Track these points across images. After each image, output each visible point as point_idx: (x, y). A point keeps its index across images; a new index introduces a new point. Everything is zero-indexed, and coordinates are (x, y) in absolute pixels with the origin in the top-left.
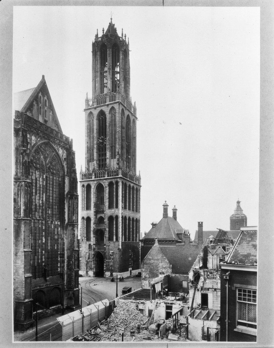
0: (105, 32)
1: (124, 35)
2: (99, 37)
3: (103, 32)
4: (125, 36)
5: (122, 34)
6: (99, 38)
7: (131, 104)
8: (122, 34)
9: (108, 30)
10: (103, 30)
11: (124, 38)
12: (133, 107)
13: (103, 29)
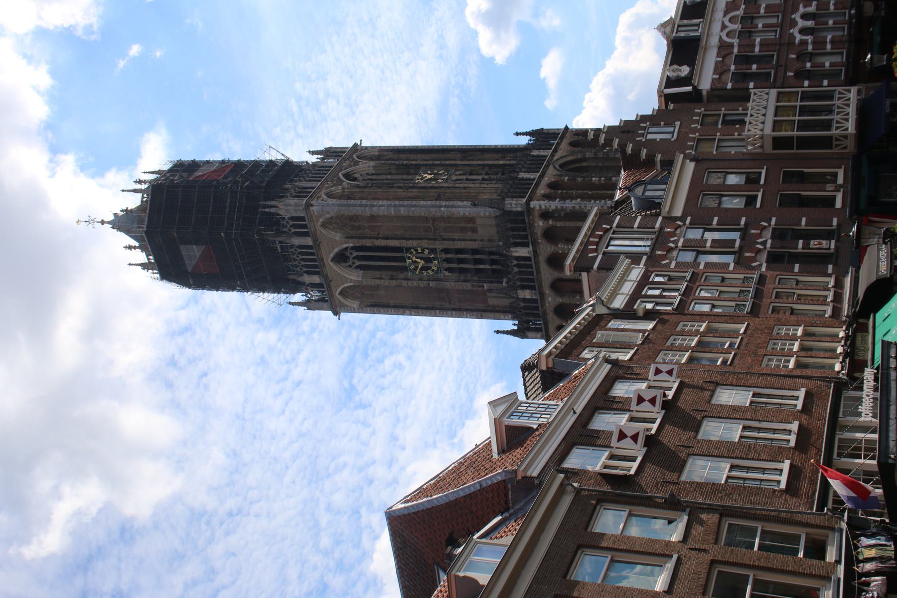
0: (135, 243)
1: (138, 186)
2: (146, 261)
3: (135, 248)
4: (140, 182)
5: (135, 191)
6: (149, 259)
7: (314, 165)
8: (135, 191)
9: (128, 232)
10: (130, 247)
11: (144, 186)
12: (323, 159)
13: (126, 247)
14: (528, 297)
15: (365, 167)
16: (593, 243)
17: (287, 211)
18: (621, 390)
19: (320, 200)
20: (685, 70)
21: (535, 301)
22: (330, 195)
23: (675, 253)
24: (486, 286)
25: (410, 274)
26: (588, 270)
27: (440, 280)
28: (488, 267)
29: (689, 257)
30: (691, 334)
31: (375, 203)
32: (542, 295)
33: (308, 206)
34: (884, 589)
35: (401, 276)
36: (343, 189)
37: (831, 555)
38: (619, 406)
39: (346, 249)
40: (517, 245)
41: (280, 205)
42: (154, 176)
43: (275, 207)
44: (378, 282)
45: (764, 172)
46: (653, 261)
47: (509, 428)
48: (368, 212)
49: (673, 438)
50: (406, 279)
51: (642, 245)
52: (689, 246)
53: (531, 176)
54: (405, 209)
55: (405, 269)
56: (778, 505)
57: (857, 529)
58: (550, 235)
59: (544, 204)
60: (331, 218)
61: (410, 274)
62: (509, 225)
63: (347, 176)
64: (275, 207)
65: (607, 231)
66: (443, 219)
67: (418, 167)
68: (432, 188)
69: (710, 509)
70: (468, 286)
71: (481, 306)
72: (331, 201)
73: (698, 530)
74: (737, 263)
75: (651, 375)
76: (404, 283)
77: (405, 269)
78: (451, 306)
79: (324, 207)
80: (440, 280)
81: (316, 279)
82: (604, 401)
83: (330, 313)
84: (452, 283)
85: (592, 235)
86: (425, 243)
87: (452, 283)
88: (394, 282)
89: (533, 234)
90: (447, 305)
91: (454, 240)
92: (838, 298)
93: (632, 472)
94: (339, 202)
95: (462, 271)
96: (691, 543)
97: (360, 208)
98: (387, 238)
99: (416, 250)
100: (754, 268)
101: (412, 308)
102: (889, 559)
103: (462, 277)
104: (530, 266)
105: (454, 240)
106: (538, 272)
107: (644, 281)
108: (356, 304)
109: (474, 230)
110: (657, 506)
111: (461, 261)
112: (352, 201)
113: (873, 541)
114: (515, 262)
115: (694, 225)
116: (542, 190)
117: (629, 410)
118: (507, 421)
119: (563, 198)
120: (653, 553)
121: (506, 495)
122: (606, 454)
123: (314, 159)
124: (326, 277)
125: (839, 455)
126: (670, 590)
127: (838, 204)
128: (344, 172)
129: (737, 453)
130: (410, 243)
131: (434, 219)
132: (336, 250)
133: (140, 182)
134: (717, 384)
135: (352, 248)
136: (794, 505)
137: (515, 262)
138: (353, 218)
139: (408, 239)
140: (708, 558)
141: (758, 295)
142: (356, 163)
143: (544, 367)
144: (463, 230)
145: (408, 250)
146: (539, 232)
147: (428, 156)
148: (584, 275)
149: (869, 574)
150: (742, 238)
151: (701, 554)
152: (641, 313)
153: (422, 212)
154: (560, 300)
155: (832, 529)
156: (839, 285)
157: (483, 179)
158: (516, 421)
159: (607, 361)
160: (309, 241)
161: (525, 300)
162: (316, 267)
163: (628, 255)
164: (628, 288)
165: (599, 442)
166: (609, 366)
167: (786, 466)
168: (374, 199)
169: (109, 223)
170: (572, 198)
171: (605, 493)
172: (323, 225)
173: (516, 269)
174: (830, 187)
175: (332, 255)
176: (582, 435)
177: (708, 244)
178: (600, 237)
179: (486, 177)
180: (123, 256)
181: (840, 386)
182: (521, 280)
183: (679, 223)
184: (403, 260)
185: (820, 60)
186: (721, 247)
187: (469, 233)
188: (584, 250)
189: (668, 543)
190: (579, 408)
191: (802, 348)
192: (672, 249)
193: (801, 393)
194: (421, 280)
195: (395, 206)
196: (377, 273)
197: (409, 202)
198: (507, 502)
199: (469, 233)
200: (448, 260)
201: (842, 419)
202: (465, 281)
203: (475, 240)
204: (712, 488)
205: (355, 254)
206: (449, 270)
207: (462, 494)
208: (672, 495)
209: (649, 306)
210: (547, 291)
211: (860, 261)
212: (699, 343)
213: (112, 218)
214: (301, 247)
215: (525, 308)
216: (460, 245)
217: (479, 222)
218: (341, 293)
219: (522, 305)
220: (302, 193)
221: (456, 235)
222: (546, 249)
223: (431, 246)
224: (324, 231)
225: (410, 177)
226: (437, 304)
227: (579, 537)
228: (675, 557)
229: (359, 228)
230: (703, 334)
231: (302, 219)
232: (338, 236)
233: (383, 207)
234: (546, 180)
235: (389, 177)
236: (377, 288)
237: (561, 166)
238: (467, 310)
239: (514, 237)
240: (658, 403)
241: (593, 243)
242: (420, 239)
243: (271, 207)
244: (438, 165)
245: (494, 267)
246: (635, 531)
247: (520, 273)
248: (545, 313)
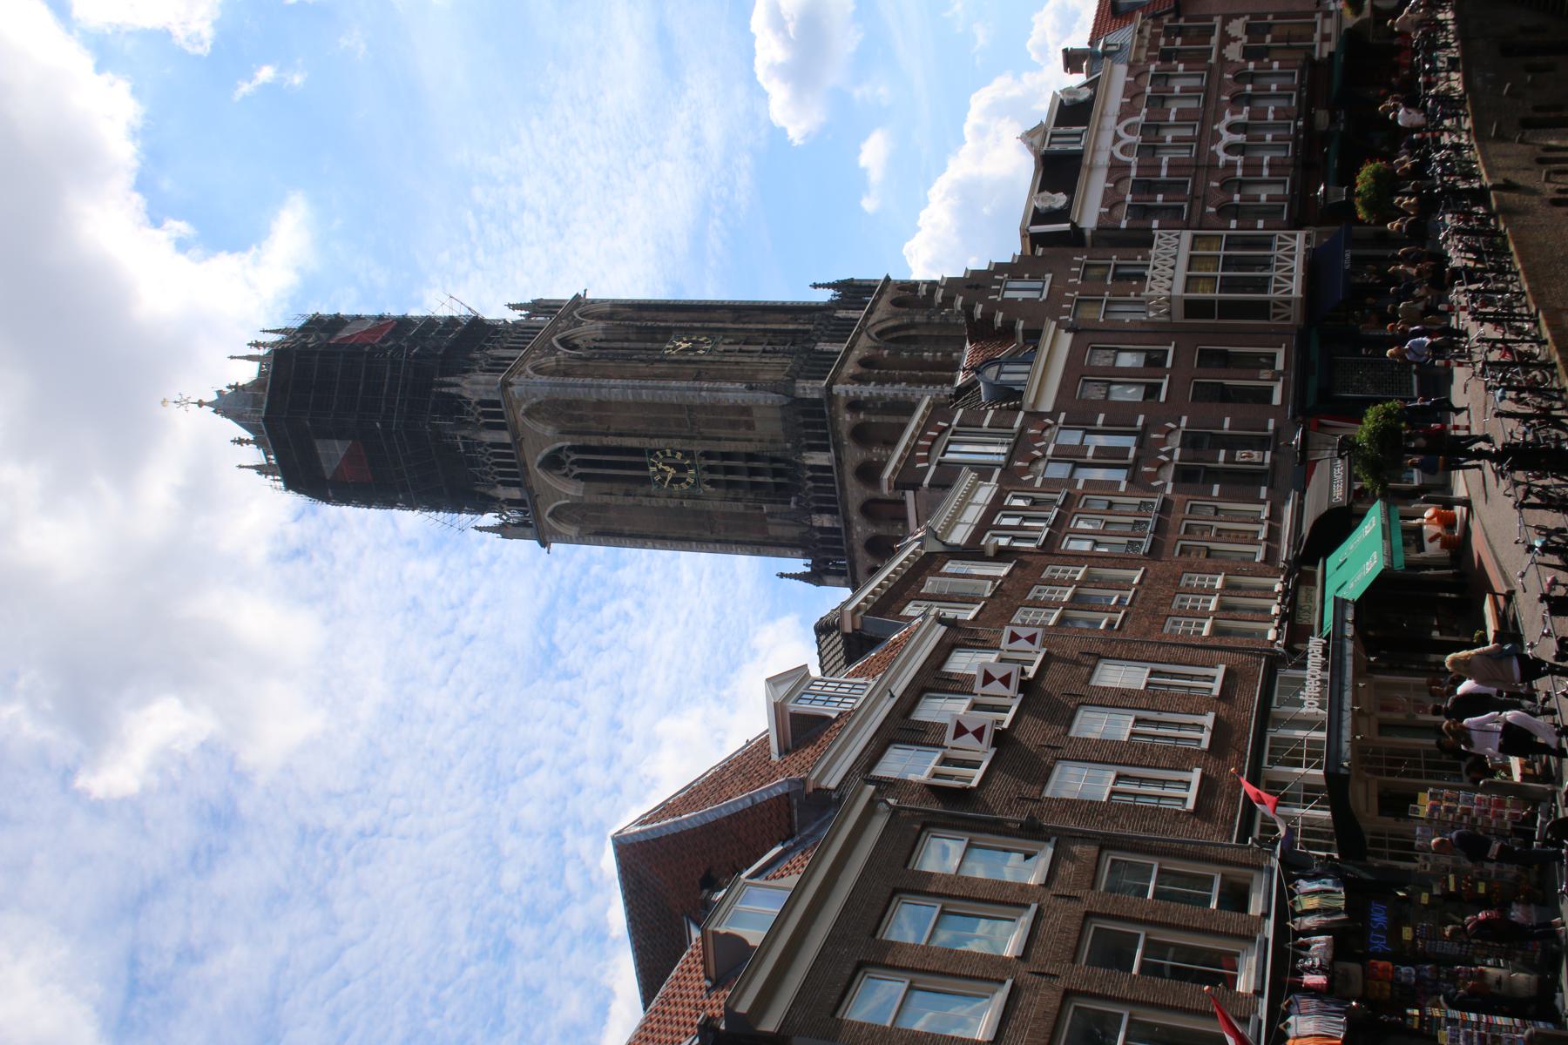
0: (248, 436)
1: (255, 352)
2: (264, 462)
3: (248, 442)
4: (257, 345)
5: (250, 358)
7: (516, 324)
8: (250, 358)
9: (238, 418)
10: (240, 442)
11: (262, 352)
12: (528, 316)
14: (827, 524)
16: (923, 448)
17: (474, 392)
18: (963, 663)
19: (523, 377)
20: (1060, 200)
22: (538, 370)
23: (1041, 465)
24: (765, 508)
25: (654, 487)
26: (916, 486)
27: (697, 498)
28: (769, 480)
29: (1059, 471)
30: (1063, 583)
31: (605, 382)
32: (848, 522)
33: (506, 385)
34: (1329, 954)
35: (641, 490)
36: (558, 361)
37: (1256, 906)
38: (958, 686)
39: (561, 449)
40: (812, 448)
42: (277, 337)
43: (457, 385)
44: (606, 499)
45: (1171, 350)
46: (1010, 477)
47: (795, 717)
48: (594, 396)
49: (1034, 734)
50: (648, 495)
51: (996, 452)
52: (1062, 454)
53: (834, 347)
54: (650, 391)
55: (647, 480)
56: (1182, 834)
57: (1295, 867)
58: (861, 435)
59: (853, 389)
60: (539, 403)
61: (654, 487)
62: (801, 420)
63: (564, 342)
64: (457, 385)
65: (943, 430)
66: (703, 407)
67: (668, 331)
68: (689, 362)
69: (1085, 838)
70: (739, 507)
71: (756, 537)
72: (538, 379)
73: (1068, 869)
74: (1131, 480)
75: (1004, 643)
76: (646, 501)
77: (647, 480)
78: (714, 536)
79: (529, 386)
80: (697, 498)
81: (516, 493)
82: (934, 680)
83: (535, 543)
84: (717, 503)
85: (922, 436)
86: (676, 443)
87: (715, 502)
88: (630, 500)
90: (707, 534)
91: (719, 439)
92: (1274, 534)
93: (974, 784)
94: (551, 380)
95: (730, 485)
96: (1057, 888)
97: (580, 388)
98: (621, 435)
99: (664, 453)
100: (1155, 490)
101: (657, 538)
102: (1337, 911)
103: (731, 494)
104: (831, 480)
105: (719, 439)
106: (842, 484)
107: (996, 505)
108: (573, 531)
109: (750, 426)
110: (1008, 833)
111: (729, 470)
112: (571, 380)
113: (1315, 886)
114: (810, 474)
115: (1069, 424)
116: (850, 368)
117: (971, 694)
118: (793, 707)
119: (881, 381)
120: (1001, 900)
121: (790, 816)
122: (937, 756)
123: (515, 316)
124: (530, 490)
125: (1271, 761)
126: (1024, 956)
127: (1277, 399)
128: (559, 336)
129: (1126, 757)
131: (691, 408)
132: (546, 451)
133: (257, 345)
134: (1099, 657)
135: (573, 449)
136: (1207, 833)
137: (810, 474)
138: (569, 404)
139: (652, 437)
140: (1081, 908)
141: (1160, 528)
142: (578, 324)
143: (848, 629)
144: (733, 425)
145: (652, 452)
146: (845, 431)
147: (683, 316)
148: (910, 494)
149: (1308, 932)
150: (1139, 446)
151: (1072, 904)
152: (991, 552)
154: (873, 530)
155: (1259, 868)
156: (1275, 516)
157: (764, 351)
158: (805, 707)
159: (940, 620)
160: (505, 437)
161: (822, 529)
162: (516, 475)
163: (974, 466)
164: (973, 514)
165: (927, 739)
166: (944, 629)
167: (1195, 776)
168: (603, 376)
169: (210, 404)
170: (894, 381)
171: (934, 813)
172: (527, 414)
173: (811, 484)
174: (1265, 374)
175: (539, 458)
176: (904, 728)
177: (1090, 453)
178: (934, 440)
179: (769, 348)
180: (234, 452)
181: (1274, 663)
183: (1048, 421)
184: (644, 467)
185: (1252, 191)
186: (1108, 458)
187: (742, 430)
188: (909, 460)
189: (1024, 888)
190: (899, 689)
191: (1222, 607)
192: (1037, 459)
193: (1219, 672)
194: (670, 497)
195: (633, 388)
196: (605, 486)
197: (655, 383)
198: (790, 825)
199: (742, 430)
200: (710, 469)
201: (1276, 709)
202: (736, 500)
203: (750, 440)
204: (1089, 808)
205: (574, 457)
206: (712, 483)
207: (725, 813)
208: (1031, 818)
209: (1003, 542)
211: (1306, 482)
212: (1074, 596)
213: (215, 397)
214: (493, 445)
215: (822, 541)
217: (757, 413)
218: (552, 515)
219: (818, 536)
220: (497, 365)
221: (722, 433)
222: (855, 455)
223: (685, 448)
224: (528, 423)
225: (656, 345)
226: (693, 533)
227: (895, 878)
228: (1034, 907)
229: (581, 419)
230: (1081, 584)
231: (496, 404)
232: (549, 430)
233: (615, 389)
234: (856, 354)
235: (626, 344)
236: (605, 507)
237: (880, 334)
238: (737, 543)
239: (808, 436)
240: (1014, 682)
241: (923, 448)
242: (670, 437)
243: (451, 385)
244: (697, 329)
245: (778, 480)
246: (981, 868)
247: (816, 489)
248: (851, 550)
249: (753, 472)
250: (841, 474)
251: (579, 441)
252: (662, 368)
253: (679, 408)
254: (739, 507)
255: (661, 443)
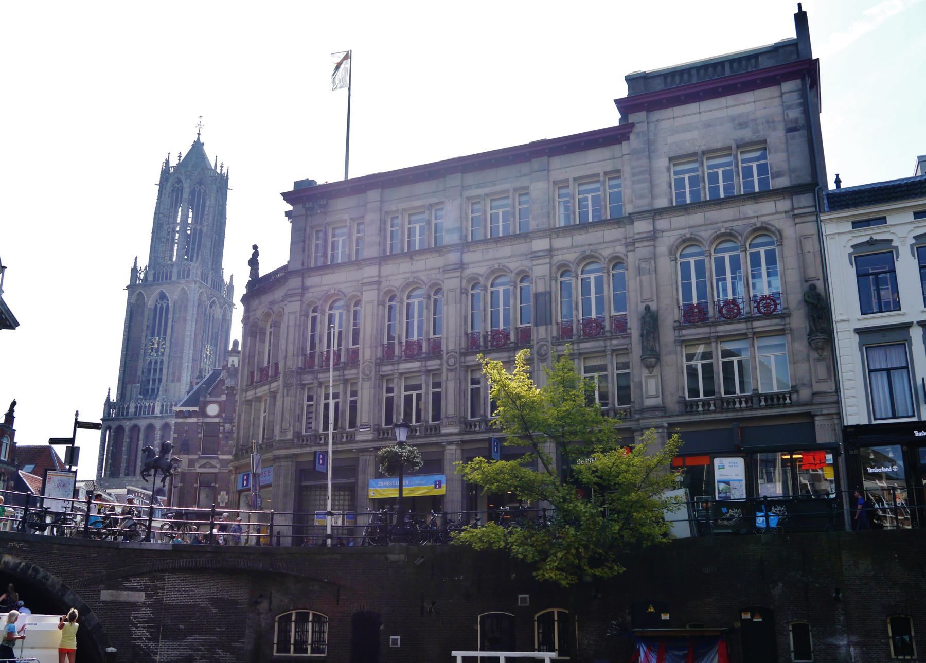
0: (182, 159)
10: (180, 157)
15: (218, 312)
21: (127, 413)
22: (201, 294)
32: (131, 419)
33: (195, 282)
35: (149, 333)
40: (162, 406)
41: (197, 264)
44: (146, 318)
48: (189, 318)
54: (188, 341)
67: (216, 345)
76: (144, 334)
77: (153, 336)
81: (150, 278)
83: (128, 283)
86: (167, 350)
89: (168, 417)
95: (149, 370)
97: (191, 313)
103: (145, 370)
109: (173, 381)
130: (168, 341)
131: (181, 357)
138: (186, 306)
145: (164, 339)
146: (168, 420)
153: (186, 351)
160: (174, 278)
161: (128, 408)
168: (197, 321)
172: (183, 289)
182: (141, 407)
184: (159, 335)
196: (151, 317)
200: (156, 362)
210: (133, 422)
214: (171, 272)
216: (165, 371)
222: (158, 424)
224: (179, 289)
231: (188, 277)
247: (145, 407)
248: (119, 420)
249: (154, 380)
250: (150, 418)
251: (171, 309)
252: (199, 346)
253: (182, 353)
254: (139, 373)
255: (168, 341)
